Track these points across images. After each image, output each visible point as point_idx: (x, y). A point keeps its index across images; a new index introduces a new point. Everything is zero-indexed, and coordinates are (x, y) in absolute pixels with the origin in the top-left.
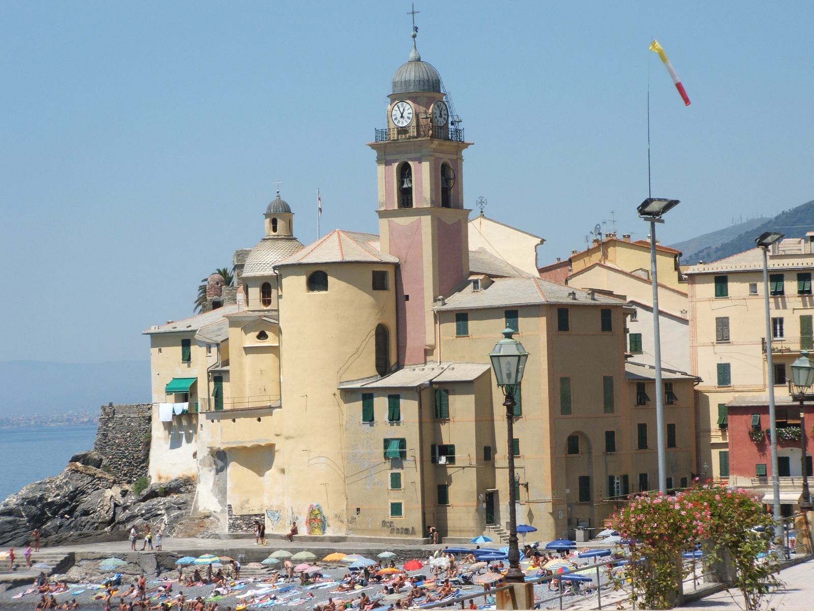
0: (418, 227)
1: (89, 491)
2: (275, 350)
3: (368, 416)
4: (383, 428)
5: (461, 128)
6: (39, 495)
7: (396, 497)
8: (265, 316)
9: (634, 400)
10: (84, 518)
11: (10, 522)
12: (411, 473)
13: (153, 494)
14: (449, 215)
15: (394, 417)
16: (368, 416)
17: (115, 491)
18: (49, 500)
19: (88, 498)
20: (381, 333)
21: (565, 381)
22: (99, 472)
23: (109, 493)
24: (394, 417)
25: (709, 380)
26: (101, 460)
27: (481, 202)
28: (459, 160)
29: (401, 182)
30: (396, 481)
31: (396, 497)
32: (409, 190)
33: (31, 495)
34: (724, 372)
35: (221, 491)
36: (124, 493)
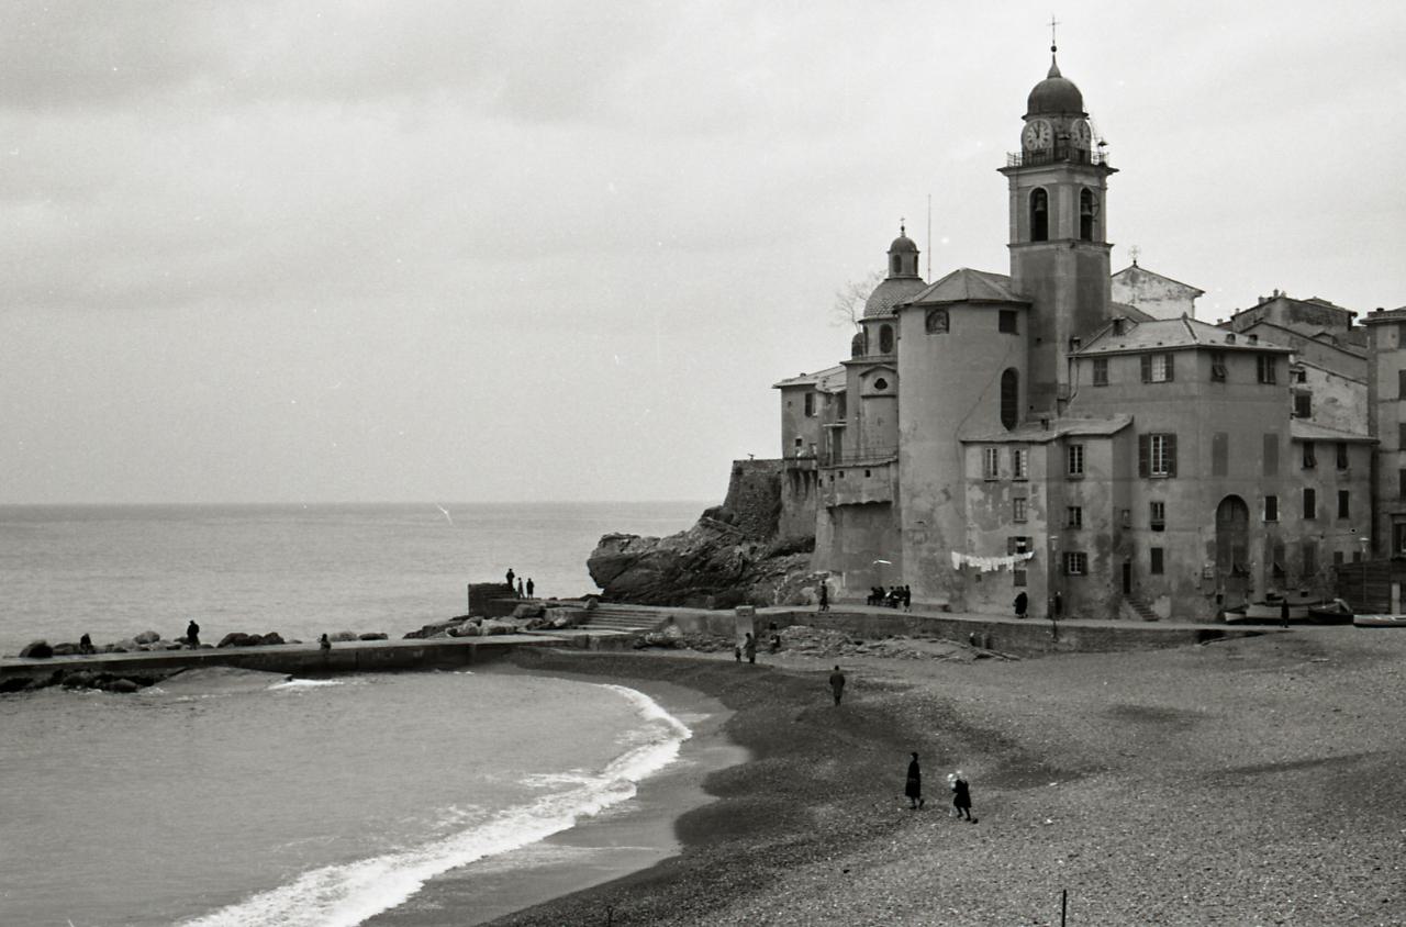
1: (719, 547)
2: (894, 396)
5: (1105, 152)
6: (672, 549)
8: (885, 363)
9: (1302, 466)
10: (712, 574)
11: (647, 575)
14: (1090, 250)
17: (744, 549)
18: (682, 554)
19: (718, 554)
20: (1009, 377)
22: (729, 528)
23: (738, 550)
26: (732, 516)
27: (1135, 252)
28: (1103, 188)
33: (665, 548)
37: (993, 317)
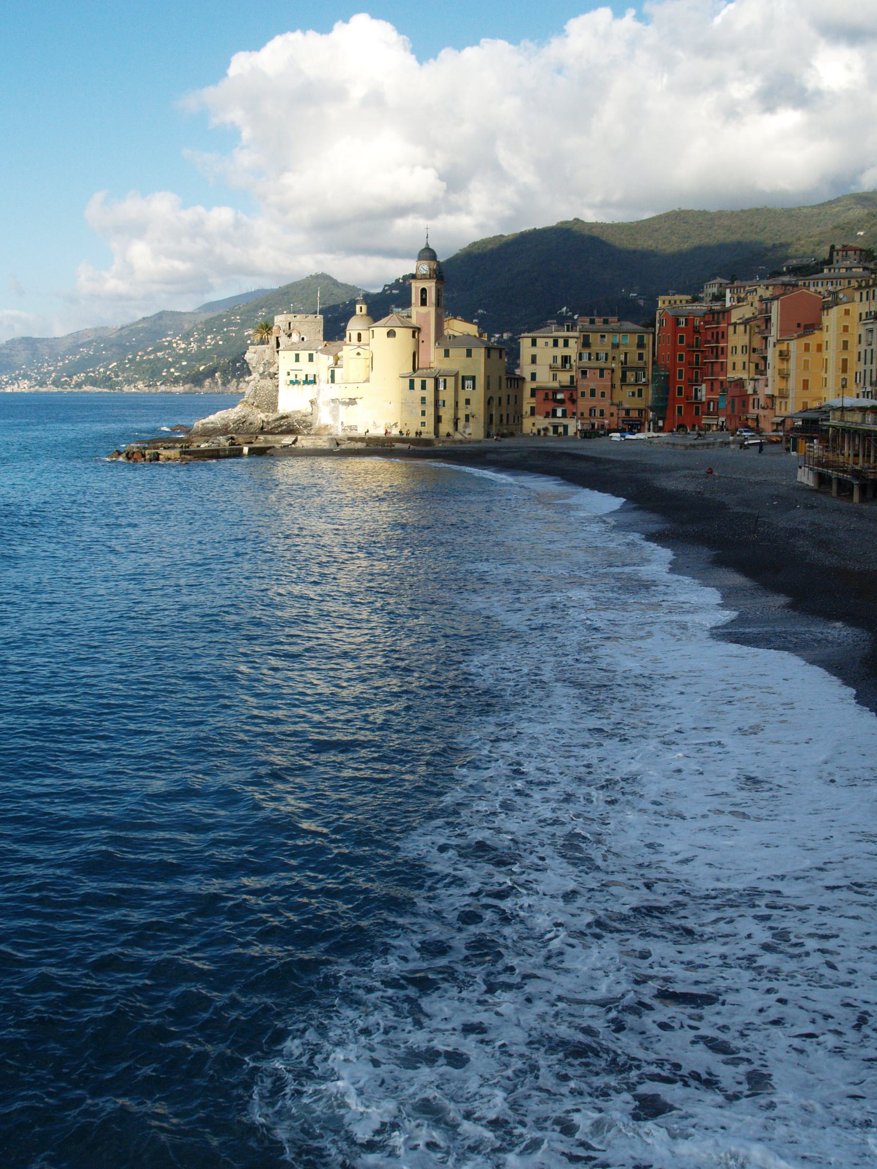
0: (429, 313)
3: (412, 387)
4: (418, 391)
7: (423, 419)
12: (430, 411)
13: (282, 418)
15: (423, 387)
16: (412, 387)
21: (488, 377)
23: (259, 416)
24: (423, 387)
25: (528, 378)
29: (422, 296)
30: (423, 413)
31: (423, 419)
32: (426, 299)
34: (533, 376)
35: (335, 417)
36: (266, 417)
37: (411, 331)
